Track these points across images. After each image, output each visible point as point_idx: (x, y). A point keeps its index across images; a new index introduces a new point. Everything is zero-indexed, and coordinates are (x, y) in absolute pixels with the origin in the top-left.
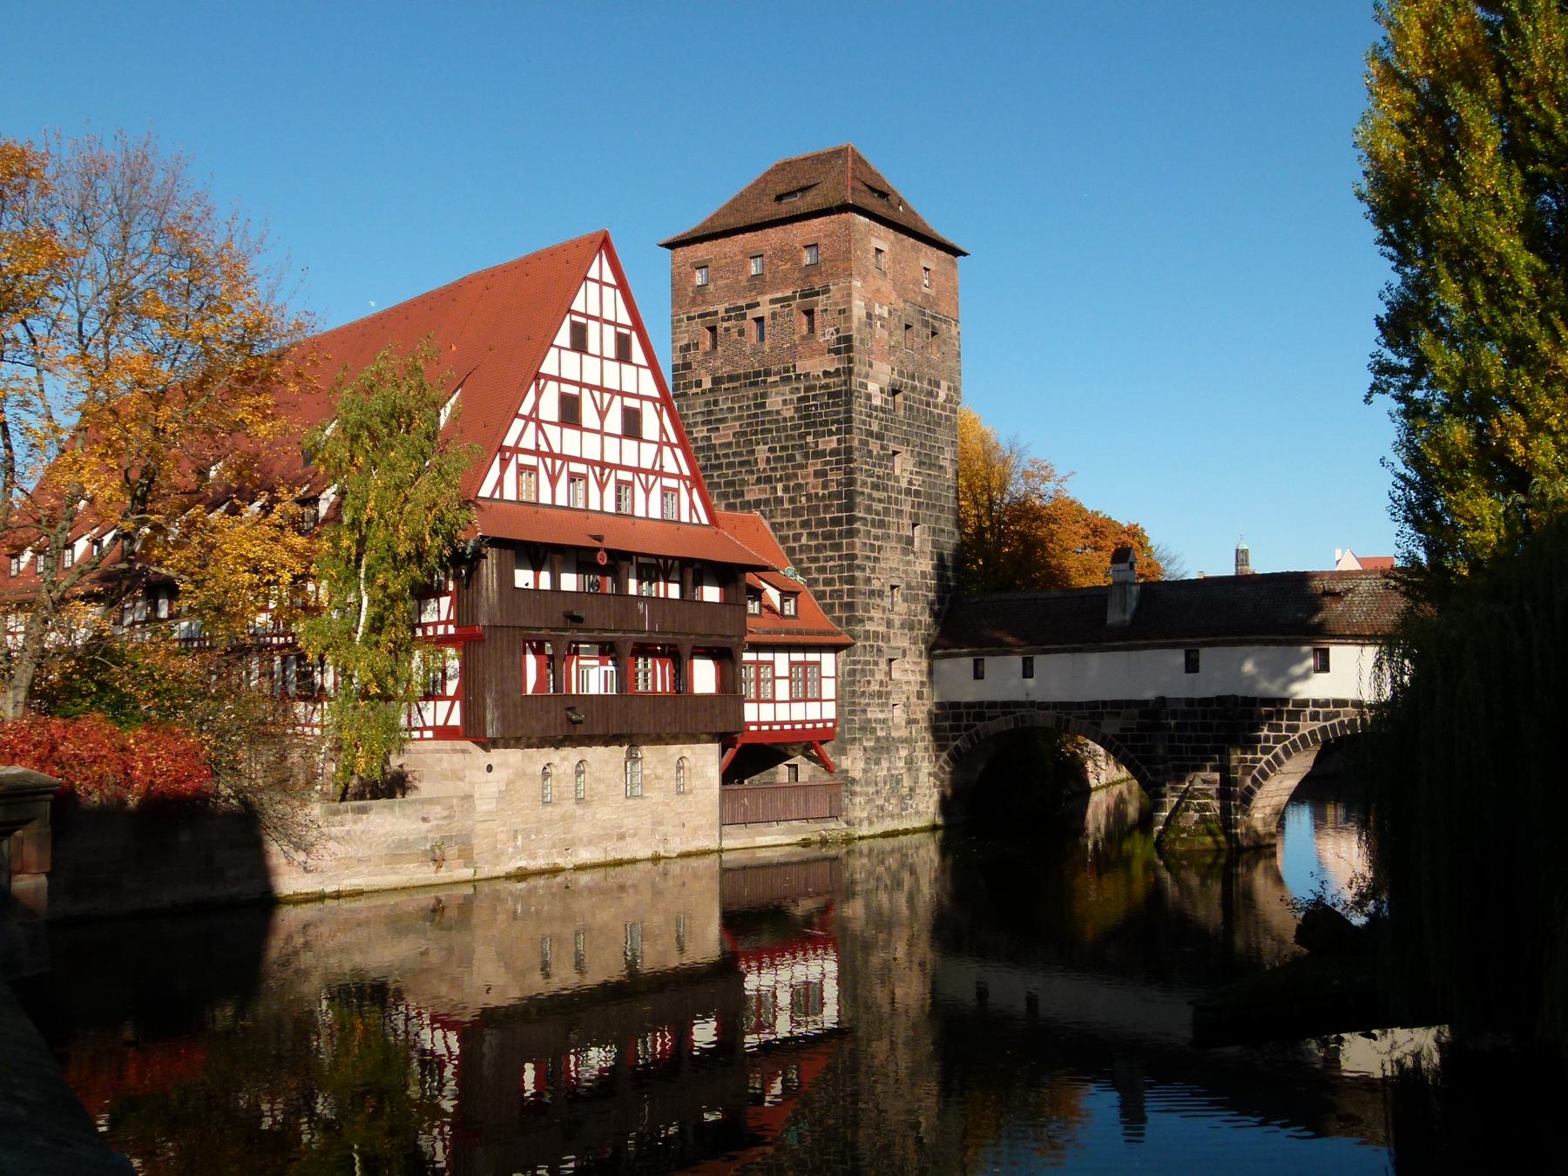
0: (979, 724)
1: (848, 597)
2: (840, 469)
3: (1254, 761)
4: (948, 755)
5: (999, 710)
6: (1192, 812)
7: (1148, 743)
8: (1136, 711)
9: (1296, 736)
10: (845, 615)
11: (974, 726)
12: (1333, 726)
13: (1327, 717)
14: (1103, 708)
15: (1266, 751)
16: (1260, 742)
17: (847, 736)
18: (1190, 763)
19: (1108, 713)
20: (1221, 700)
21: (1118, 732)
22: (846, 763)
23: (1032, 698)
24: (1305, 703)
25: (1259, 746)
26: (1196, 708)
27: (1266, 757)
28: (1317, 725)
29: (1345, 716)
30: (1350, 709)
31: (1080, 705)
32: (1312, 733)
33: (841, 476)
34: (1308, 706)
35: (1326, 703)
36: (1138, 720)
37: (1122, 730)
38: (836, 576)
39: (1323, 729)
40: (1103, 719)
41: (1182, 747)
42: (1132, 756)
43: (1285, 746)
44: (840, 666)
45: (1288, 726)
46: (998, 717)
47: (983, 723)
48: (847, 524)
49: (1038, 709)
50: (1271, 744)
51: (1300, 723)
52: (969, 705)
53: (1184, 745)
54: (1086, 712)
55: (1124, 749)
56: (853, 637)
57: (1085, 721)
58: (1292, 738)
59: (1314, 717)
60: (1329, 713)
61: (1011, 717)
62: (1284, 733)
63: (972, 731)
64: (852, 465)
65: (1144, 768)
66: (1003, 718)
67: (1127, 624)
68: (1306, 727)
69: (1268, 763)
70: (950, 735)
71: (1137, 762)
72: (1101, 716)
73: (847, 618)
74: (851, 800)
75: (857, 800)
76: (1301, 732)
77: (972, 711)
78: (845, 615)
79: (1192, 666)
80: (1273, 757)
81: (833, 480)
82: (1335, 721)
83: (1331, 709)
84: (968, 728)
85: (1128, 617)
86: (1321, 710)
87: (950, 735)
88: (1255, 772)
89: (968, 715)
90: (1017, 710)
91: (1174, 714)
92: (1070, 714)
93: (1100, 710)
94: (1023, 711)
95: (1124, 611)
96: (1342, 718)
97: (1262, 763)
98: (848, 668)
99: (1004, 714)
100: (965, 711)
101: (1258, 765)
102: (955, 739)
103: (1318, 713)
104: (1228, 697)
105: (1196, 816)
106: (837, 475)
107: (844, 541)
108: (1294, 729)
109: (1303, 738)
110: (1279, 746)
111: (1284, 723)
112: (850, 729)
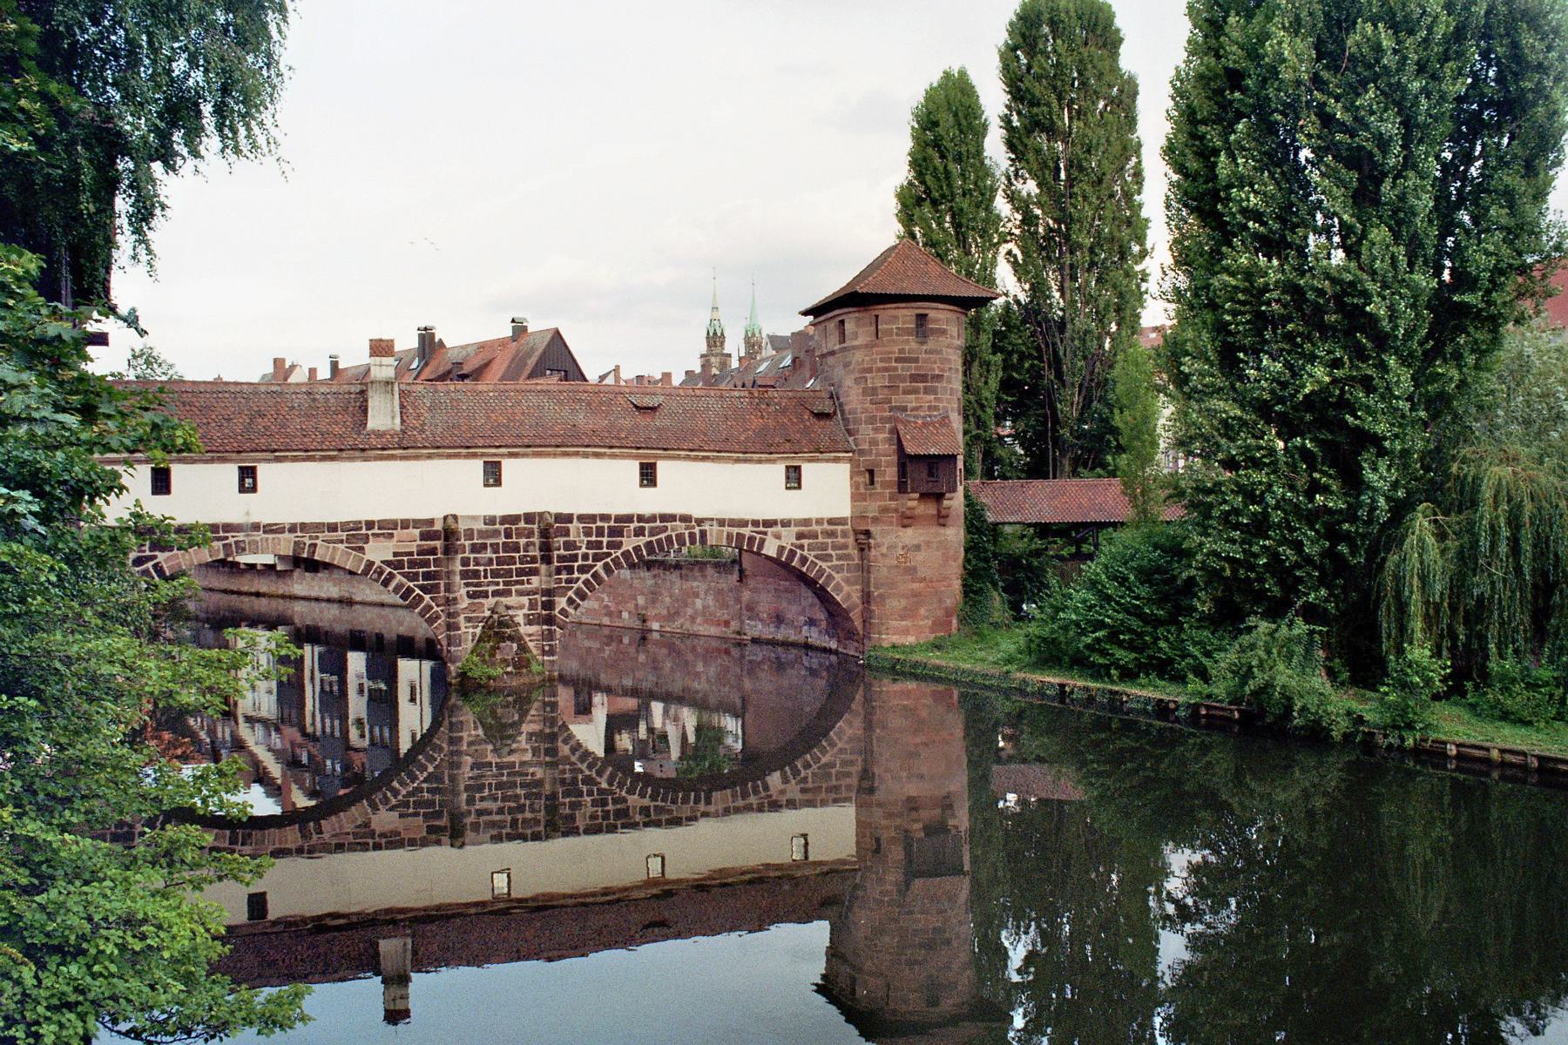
0: (161, 557)
3: (569, 581)
7: (433, 568)
8: (417, 532)
9: (619, 553)
11: (155, 557)
12: (659, 542)
15: (582, 569)
18: (491, 589)
20: (529, 518)
21: (391, 558)
23: (254, 519)
24: (629, 518)
25: (576, 564)
27: (584, 577)
28: (641, 541)
29: (673, 530)
31: (333, 527)
32: (637, 549)
35: (652, 518)
36: (419, 542)
37: (395, 554)
39: (649, 545)
41: (478, 571)
42: (411, 584)
47: (167, 554)
49: (265, 532)
50: (590, 562)
51: (624, 539)
53: (482, 568)
55: (399, 577)
59: (639, 532)
62: (605, 550)
65: (427, 597)
69: (586, 583)
71: (418, 591)
72: (366, 539)
76: (624, 548)
79: (493, 475)
80: (592, 576)
82: (663, 536)
85: (398, 420)
86: (647, 525)
88: (570, 593)
90: (229, 535)
91: (469, 534)
92: (317, 537)
94: (241, 536)
96: (669, 533)
101: (576, 586)
104: (541, 515)
108: (618, 545)
109: (626, 554)
110: (600, 564)
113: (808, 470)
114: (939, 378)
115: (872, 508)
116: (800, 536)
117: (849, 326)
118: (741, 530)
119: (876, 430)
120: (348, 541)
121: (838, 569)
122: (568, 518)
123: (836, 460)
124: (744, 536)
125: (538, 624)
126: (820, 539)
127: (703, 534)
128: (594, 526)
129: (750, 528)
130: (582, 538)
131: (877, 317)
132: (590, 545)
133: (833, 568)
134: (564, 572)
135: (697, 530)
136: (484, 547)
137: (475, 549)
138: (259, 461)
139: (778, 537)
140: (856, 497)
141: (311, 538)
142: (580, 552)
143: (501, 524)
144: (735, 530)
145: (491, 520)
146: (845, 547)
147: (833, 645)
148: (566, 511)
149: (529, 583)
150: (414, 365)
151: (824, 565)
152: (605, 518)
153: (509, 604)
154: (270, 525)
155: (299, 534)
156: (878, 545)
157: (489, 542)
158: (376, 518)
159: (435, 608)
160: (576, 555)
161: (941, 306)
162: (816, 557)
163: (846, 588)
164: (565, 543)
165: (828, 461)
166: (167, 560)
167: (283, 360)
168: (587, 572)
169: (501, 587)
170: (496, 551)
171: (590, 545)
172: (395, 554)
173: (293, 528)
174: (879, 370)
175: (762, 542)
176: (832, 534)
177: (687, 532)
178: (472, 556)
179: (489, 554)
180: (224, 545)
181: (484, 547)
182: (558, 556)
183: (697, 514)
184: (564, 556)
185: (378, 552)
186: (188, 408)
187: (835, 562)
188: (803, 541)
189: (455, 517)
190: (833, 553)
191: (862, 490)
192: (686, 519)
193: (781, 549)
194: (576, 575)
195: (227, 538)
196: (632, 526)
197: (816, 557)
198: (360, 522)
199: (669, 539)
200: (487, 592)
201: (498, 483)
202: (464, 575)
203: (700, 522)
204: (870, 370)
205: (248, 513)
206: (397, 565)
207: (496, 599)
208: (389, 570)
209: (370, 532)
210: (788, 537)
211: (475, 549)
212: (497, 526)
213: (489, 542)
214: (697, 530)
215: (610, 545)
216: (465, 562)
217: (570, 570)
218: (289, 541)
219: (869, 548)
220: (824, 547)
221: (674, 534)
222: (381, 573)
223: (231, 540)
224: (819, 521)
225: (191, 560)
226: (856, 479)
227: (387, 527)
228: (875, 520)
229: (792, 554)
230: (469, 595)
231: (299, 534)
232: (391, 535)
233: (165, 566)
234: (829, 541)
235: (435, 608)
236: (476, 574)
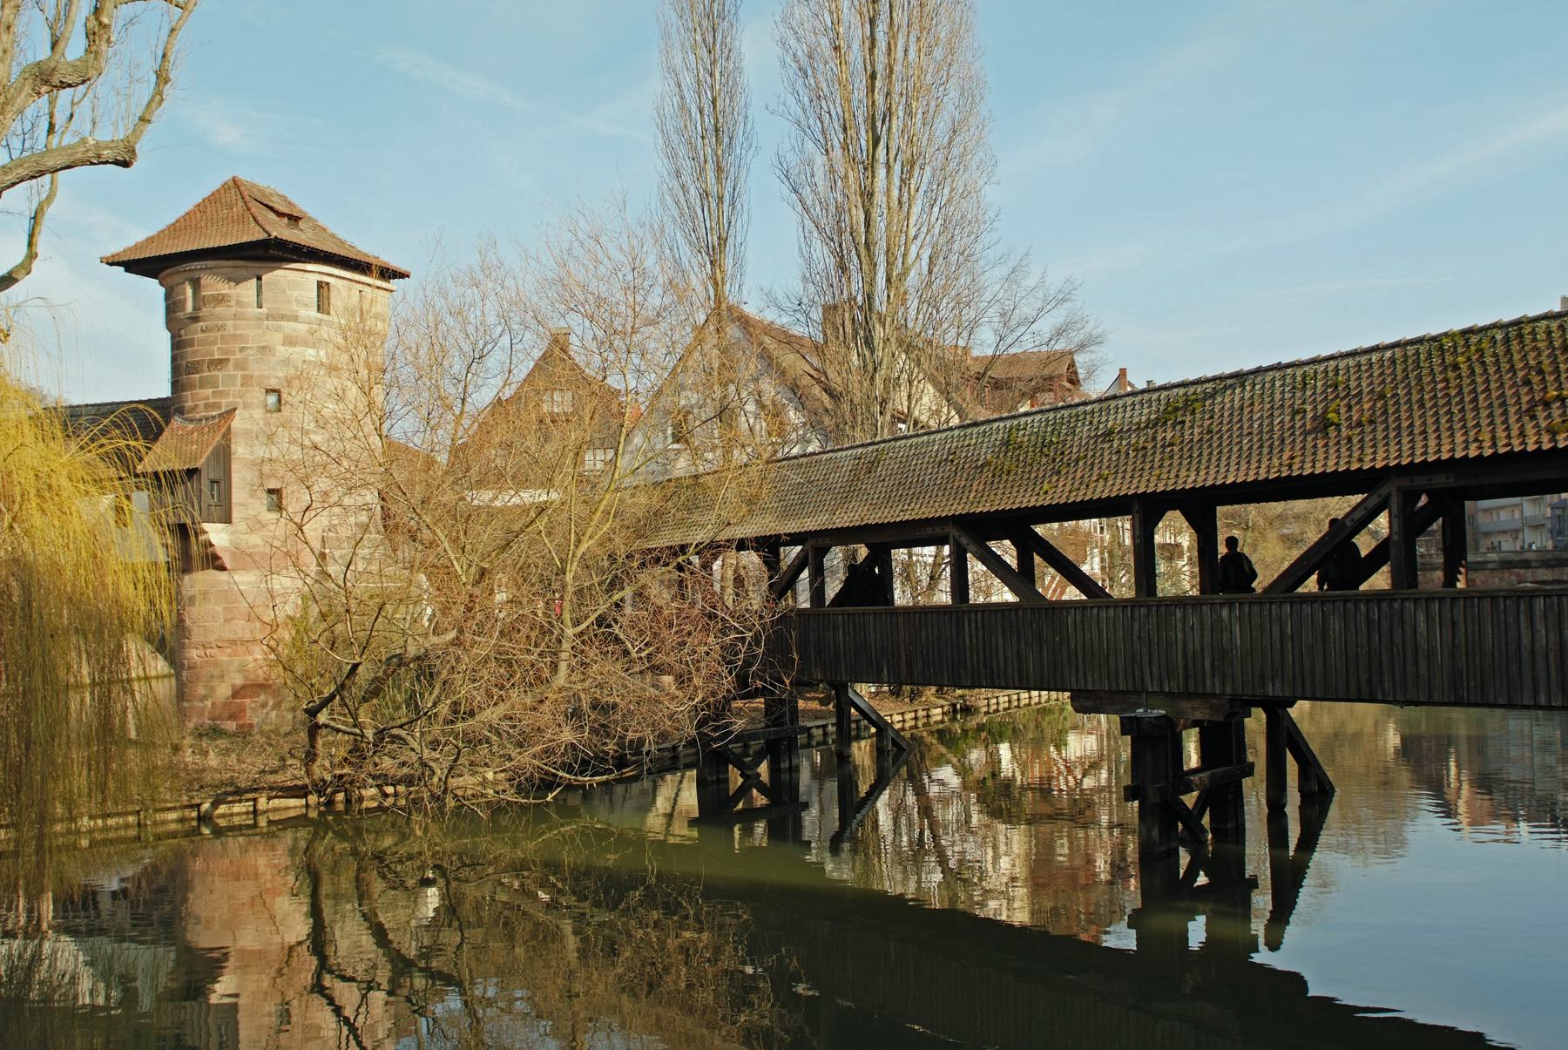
114: (220, 363)
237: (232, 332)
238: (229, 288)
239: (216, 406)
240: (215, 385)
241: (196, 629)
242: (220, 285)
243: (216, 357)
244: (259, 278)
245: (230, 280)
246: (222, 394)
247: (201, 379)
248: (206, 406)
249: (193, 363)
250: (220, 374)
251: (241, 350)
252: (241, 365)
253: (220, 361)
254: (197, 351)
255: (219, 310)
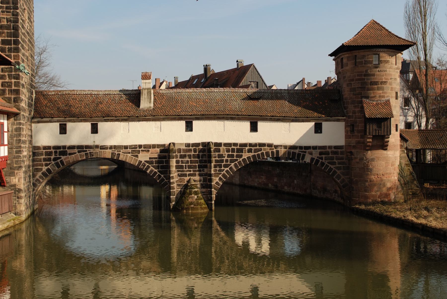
0: (63, 158)
1: (15, 86)
2: (7, 12)
3: (219, 171)
4: (43, 173)
5: (76, 150)
6: (193, 195)
7: (165, 164)
10: (13, 96)
12: (258, 155)
13: (256, 151)
14: (139, 148)
15: (226, 166)
16: (223, 162)
17: (15, 165)
18: (188, 173)
19: (142, 150)
21: (148, 160)
22: (14, 180)
23: (97, 143)
24: (245, 145)
25: (223, 164)
26: (191, 148)
27: (226, 169)
28: (251, 154)
29: (264, 150)
30: (266, 147)
31: (126, 147)
32: (249, 158)
33: (10, 16)
34: (247, 146)
35: (255, 145)
37: (150, 158)
38: (6, 74)
39: (254, 156)
40: (139, 153)
42: (156, 170)
43: (236, 164)
44: (10, 126)
45: (237, 155)
46: (76, 153)
47: (65, 157)
48: (14, 44)
49: (100, 149)
50: (229, 163)
51: (243, 154)
52: (56, 148)
53: (184, 165)
54: (130, 150)
55: (151, 167)
56: (19, 109)
57: (129, 155)
58: (239, 160)
59: (250, 151)
60: (257, 149)
61: (84, 153)
62: (235, 158)
63: (59, 160)
64: (18, 11)
65: (162, 176)
66: (79, 154)
67: (152, 108)
68: (245, 155)
69: (227, 171)
70: (44, 163)
72: (139, 152)
73: (14, 98)
74: (18, 201)
75: (22, 201)
76: (243, 157)
77: (58, 150)
78: (13, 96)
79: (189, 127)
80: (229, 169)
81: (4, 18)
82: (260, 152)
83: (258, 147)
84: (55, 159)
85: (152, 105)
86: (253, 148)
87: (44, 163)
88: (220, 176)
89: (56, 152)
91: (179, 150)
92: (120, 151)
93: (138, 149)
94: (92, 150)
95: (150, 102)
96: (263, 151)
97: (224, 172)
98: (15, 127)
99: (79, 152)
100: (53, 151)
101: (222, 173)
102: (47, 165)
103: (252, 149)
105: (196, 197)
106: (7, 15)
107: (12, 54)
109: (244, 160)
110: (233, 164)
111: (235, 154)
112: (17, 161)
113: (325, 125)
114: (385, 83)
115: (353, 141)
116: (321, 153)
117: (345, 61)
118: (294, 151)
119: (355, 107)
120: (131, 153)
121: (339, 168)
122: (219, 145)
123: (338, 120)
124: (295, 153)
125: (207, 188)
126: (330, 155)
127: (277, 152)
128: (230, 148)
129: (298, 150)
130: (226, 153)
131: (356, 56)
132: (229, 156)
133: (337, 168)
134: (218, 167)
135: (275, 150)
136: (184, 156)
137: (182, 157)
138: (98, 121)
139: (311, 154)
140: (347, 137)
141: (118, 151)
142: (224, 159)
143: (192, 147)
144: (292, 151)
145: (188, 145)
146: (342, 159)
147: (342, 201)
148: (218, 141)
149: (204, 171)
150: (202, 81)
151: (332, 167)
152: (235, 144)
153: (196, 179)
154: (102, 146)
155: (113, 150)
156: (356, 158)
157: (187, 154)
158: (143, 143)
159: (166, 180)
160: (223, 160)
161: (385, 50)
162: (328, 163)
163: (343, 177)
164: (218, 155)
165: (334, 121)
166: (65, 159)
167: (159, 79)
168: (227, 167)
169: (192, 172)
170: (190, 158)
171: (229, 156)
172: (150, 158)
173: (111, 147)
174: (357, 80)
175: (304, 157)
176: (336, 153)
177: (270, 151)
178: (180, 160)
179: (187, 159)
180: (85, 154)
181: (184, 156)
182: (215, 160)
183: (276, 143)
184: (218, 160)
185: (143, 157)
186: (74, 101)
187: (337, 165)
188: (322, 156)
189: (174, 144)
190: (337, 161)
191: (349, 134)
192: (270, 145)
193: (312, 159)
194: (223, 168)
195: (86, 151)
196: (247, 148)
197: (328, 163)
198: (136, 145)
199: (262, 154)
200: (186, 174)
201: (191, 130)
202: (177, 167)
203: (276, 147)
204: (353, 80)
205: (94, 142)
206: (150, 162)
207: (190, 177)
208: (147, 164)
209: (140, 149)
210: (316, 154)
211: (182, 157)
212: (191, 148)
213: (187, 154)
214: (275, 150)
215: (237, 156)
216: (177, 162)
217: (220, 166)
218: (110, 153)
219: (352, 159)
220: (332, 158)
221: (264, 152)
222: (145, 165)
223: (88, 152)
224: (330, 147)
225: (74, 159)
226: (347, 129)
227: (147, 148)
228: (354, 147)
229: (317, 161)
230: (179, 175)
231: (113, 150)
232: (148, 151)
233: (64, 161)
234: (335, 156)
235: (166, 180)
236: (182, 167)
237: (388, 73)
238: (389, 58)
239: (383, 97)
240: (382, 89)
241: (374, 169)
242: (387, 57)
243: (384, 81)
244: (396, 55)
245: (390, 55)
246: (385, 93)
247: (378, 87)
248: (380, 96)
249: (375, 82)
250: (385, 86)
251: (391, 79)
252: (391, 84)
253: (385, 82)
254: (376, 78)
255: (386, 65)
